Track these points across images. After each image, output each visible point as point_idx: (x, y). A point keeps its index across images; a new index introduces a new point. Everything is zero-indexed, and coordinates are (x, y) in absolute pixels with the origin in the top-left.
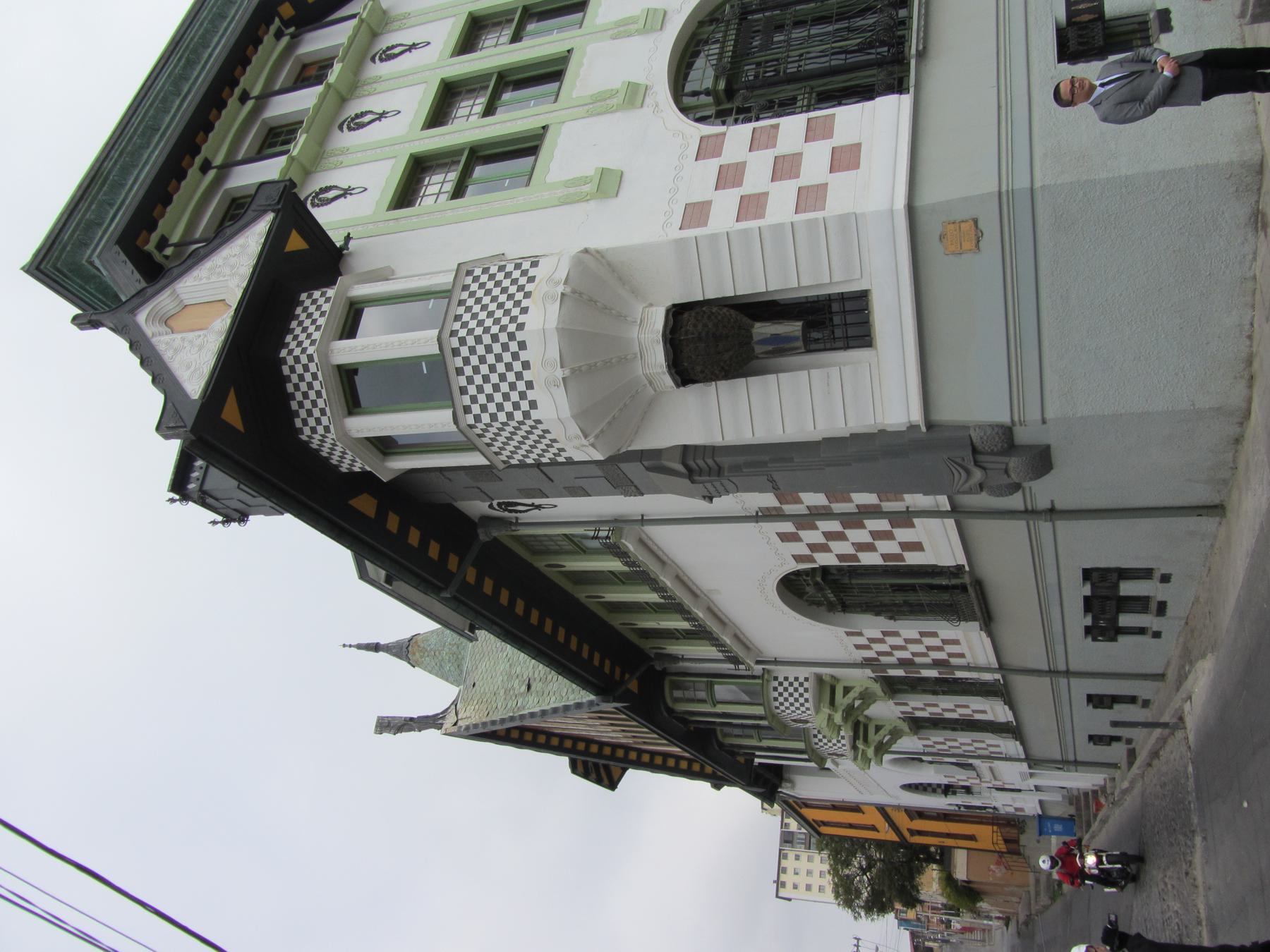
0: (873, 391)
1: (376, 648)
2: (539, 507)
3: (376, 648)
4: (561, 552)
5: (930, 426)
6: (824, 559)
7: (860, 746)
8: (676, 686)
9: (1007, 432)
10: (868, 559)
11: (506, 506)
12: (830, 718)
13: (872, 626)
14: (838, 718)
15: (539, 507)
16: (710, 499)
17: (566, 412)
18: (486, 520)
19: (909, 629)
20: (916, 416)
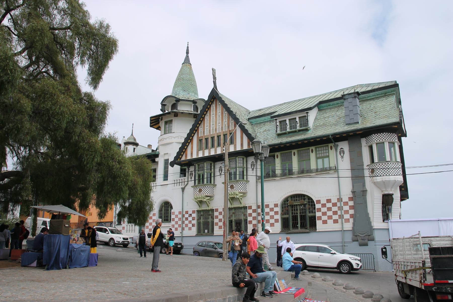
0: (377, 221)
1: (187, 53)
2: (342, 157)
3: (187, 53)
4: (316, 154)
5: (374, 229)
6: (318, 206)
7: (209, 198)
8: (243, 159)
9: (373, 240)
10: (318, 214)
11: (342, 152)
12: (237, 195)
13: (278, 209)
14: (238, 197)
15: (342, 157)
16: (353, 192)
17: (391, 179)
18: (338, 145)
19: (278, 217)
20: (375, 227)
